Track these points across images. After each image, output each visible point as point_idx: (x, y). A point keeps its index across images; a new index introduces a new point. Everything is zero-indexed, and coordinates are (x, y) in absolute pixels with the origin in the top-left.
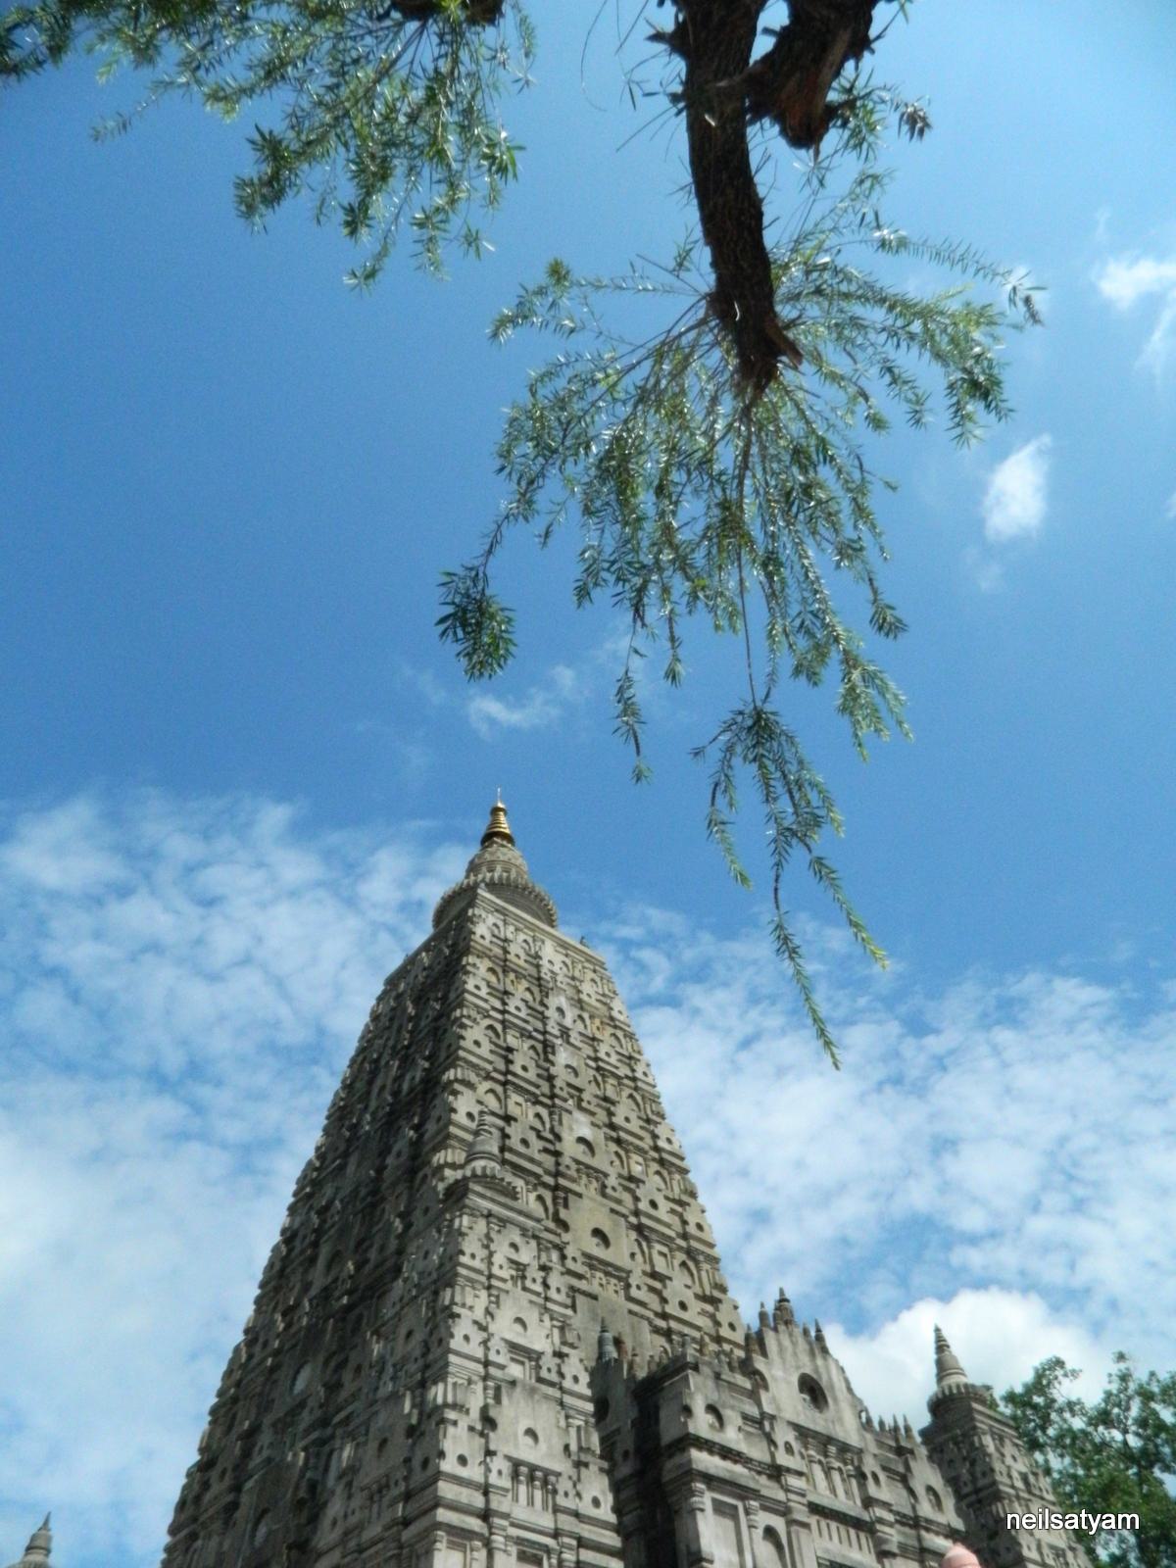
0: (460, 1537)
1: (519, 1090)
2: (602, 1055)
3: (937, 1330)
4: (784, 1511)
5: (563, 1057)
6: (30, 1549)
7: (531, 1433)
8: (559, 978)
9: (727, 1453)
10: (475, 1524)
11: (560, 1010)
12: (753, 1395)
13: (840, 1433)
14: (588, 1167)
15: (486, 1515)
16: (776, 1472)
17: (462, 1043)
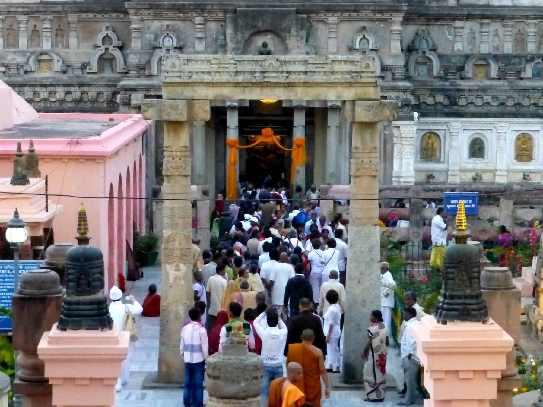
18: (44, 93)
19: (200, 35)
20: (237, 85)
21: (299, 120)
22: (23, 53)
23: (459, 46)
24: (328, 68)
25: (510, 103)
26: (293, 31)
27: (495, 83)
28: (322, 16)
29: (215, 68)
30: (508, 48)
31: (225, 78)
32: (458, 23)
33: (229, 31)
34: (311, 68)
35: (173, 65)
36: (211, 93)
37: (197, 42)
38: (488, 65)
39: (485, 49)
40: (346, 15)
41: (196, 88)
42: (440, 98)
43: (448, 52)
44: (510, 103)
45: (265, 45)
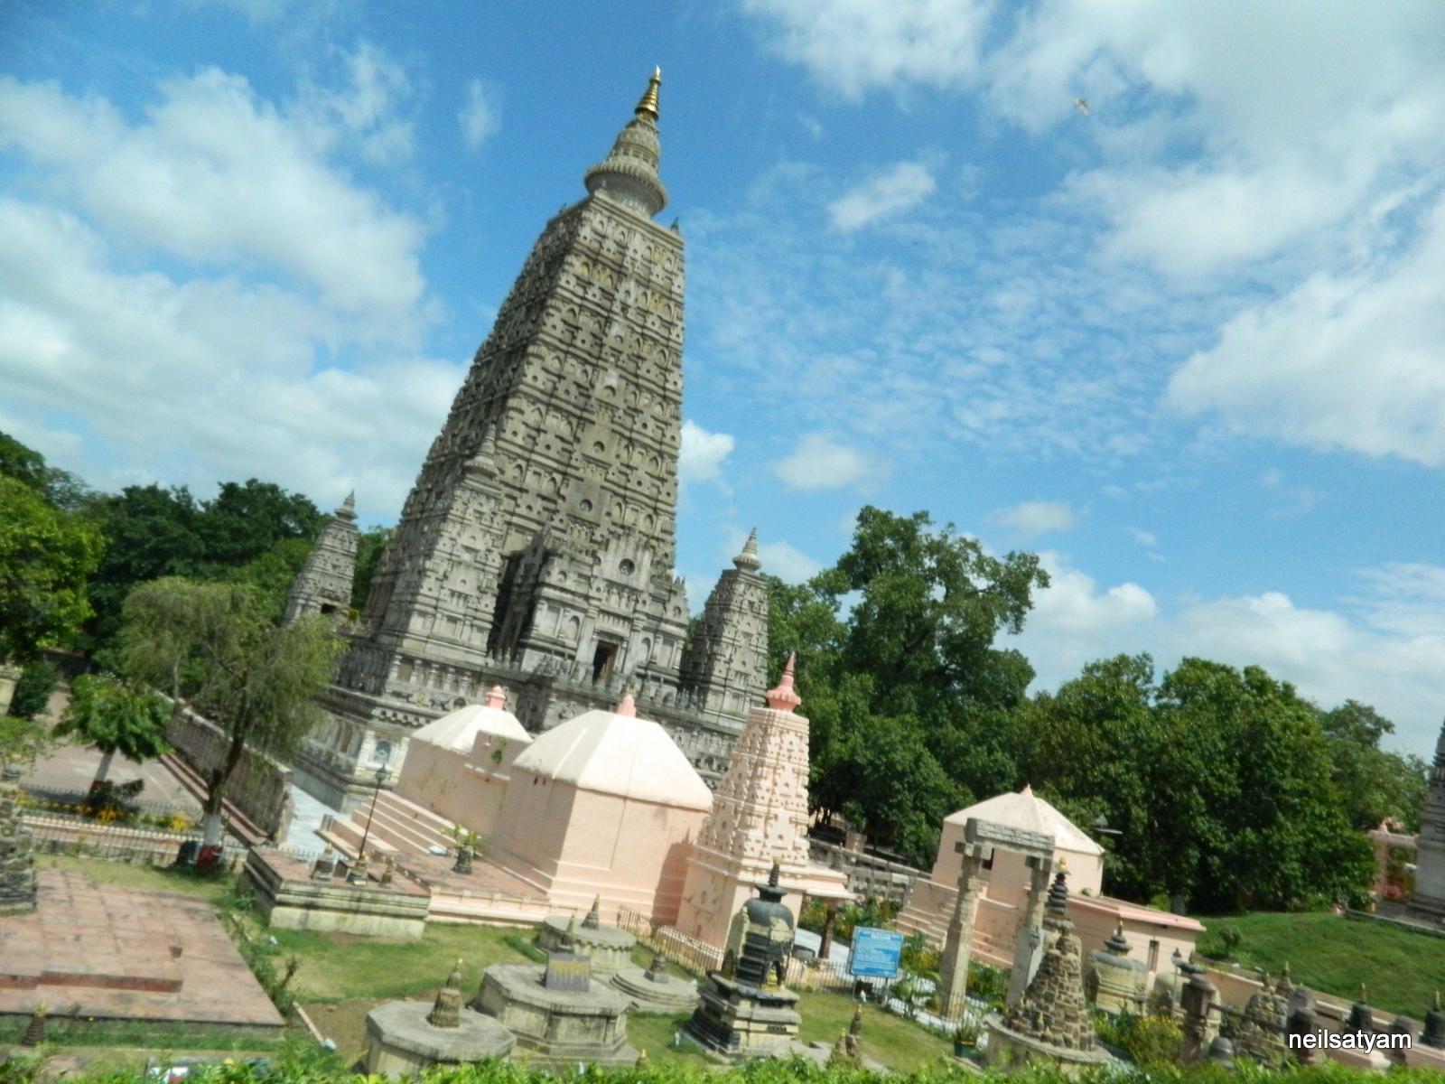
0: (423, 614)
1: (575, 356)
2: (649, 324)
4: (585, 611)
5: (616, 330)
6: (346, 503)
7: (464, 581)
8: (638, 264)
9: (563, 590)
10: (431, 610)
11: (628, 292)
12: (591, 567)
13: (634, 584)
15: (436, 608)
16: (587, 598)
17: (544, 328)
18: (389, 713)
22: (446, 695)
30: (723, 753)
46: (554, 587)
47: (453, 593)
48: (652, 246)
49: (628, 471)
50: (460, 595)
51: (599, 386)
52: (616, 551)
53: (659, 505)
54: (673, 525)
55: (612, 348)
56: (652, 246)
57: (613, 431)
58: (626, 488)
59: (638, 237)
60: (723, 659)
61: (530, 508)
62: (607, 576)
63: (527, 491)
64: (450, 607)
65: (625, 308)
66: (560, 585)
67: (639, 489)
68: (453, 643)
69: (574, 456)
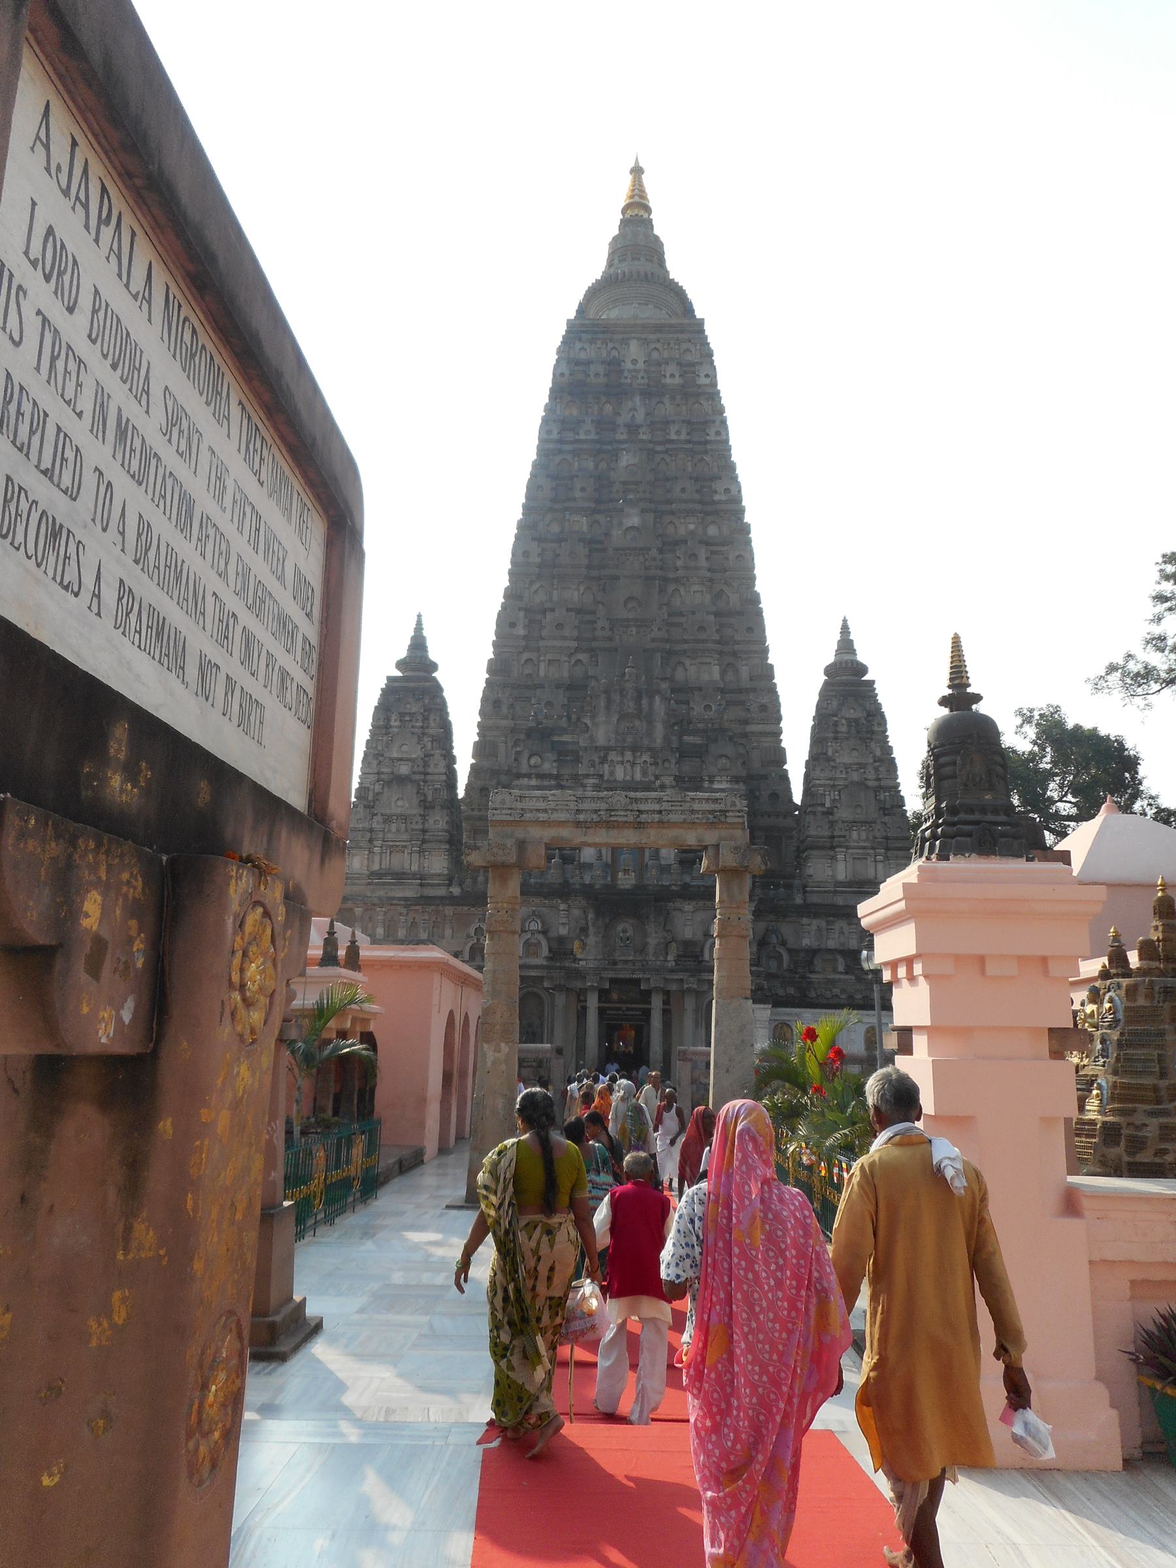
3: (845, 621)
14: (635, 549)
19: (564, 921)
20: (578, 824)
21: (657, 1003)
23: (806, 942)
24: (686, 806)
25: (858, 996)
26: (652, 918)
27: (842, 977)
28: (678, 904)
29: (552, 805)
31: (563, 816)
32: (805, 920)
33: (591, 916)
34: (665, 806)
35: (503, 802)
36: (548, 834)
37: (561, 927)
38: (836, 960)
39: (831, 944)
40: (701, 903)
41: (529, 829)
42: (791, 990)
43: (795, 947)
44: (858, 996)
45: (625, 931)
46: (529, 776)
47: (388, 819)
48: (658, 345)
49: (683, 620)
50: (398, 816)
51: (616, 533)
52: (608, 707)
53: (736, 647)
54: (771, 667)
55: (624, 483)
56: (658, 345)
57: (648, 578)
58: (686, 642)
59: (634, 346)
60: (820, 809)
61: (549, 704)
62: (601, 741)
63: (542, 687)
64: (390, 836)
65: (632, 428)
66: (533, 771)
67: (702, 636)
68: (400, 877)
69: (600, 624)
